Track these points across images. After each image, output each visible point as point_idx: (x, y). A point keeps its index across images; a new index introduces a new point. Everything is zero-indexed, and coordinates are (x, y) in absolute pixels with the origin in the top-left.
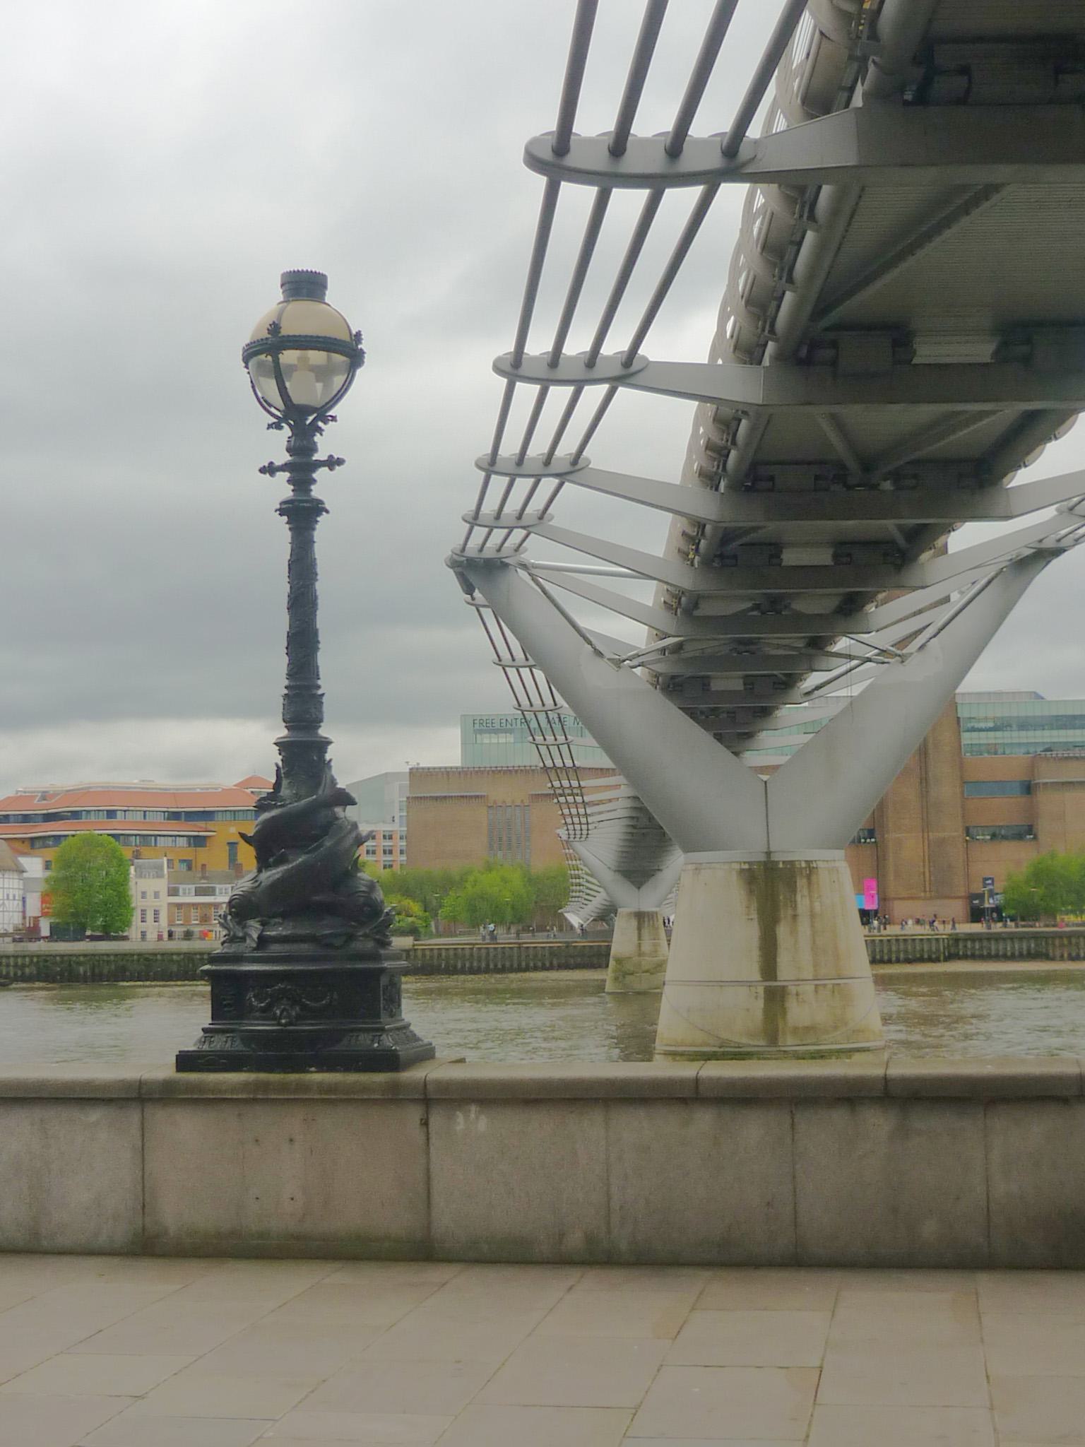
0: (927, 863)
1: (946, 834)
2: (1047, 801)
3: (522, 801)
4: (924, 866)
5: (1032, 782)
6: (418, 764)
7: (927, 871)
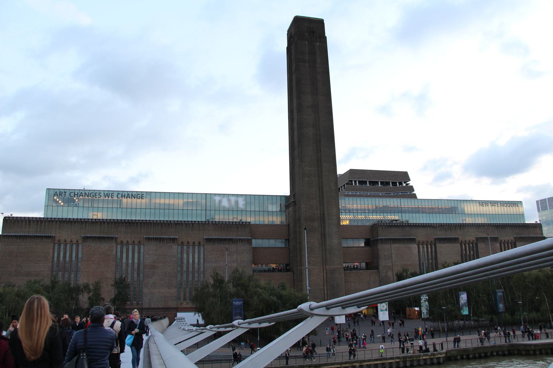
0: (325, 283)
1: (335, 266)
2: (383, 249)
3: (77, 241)
4: (324, 285)
5: (371, 239)
6: (11, 215)
7: (325, 288)
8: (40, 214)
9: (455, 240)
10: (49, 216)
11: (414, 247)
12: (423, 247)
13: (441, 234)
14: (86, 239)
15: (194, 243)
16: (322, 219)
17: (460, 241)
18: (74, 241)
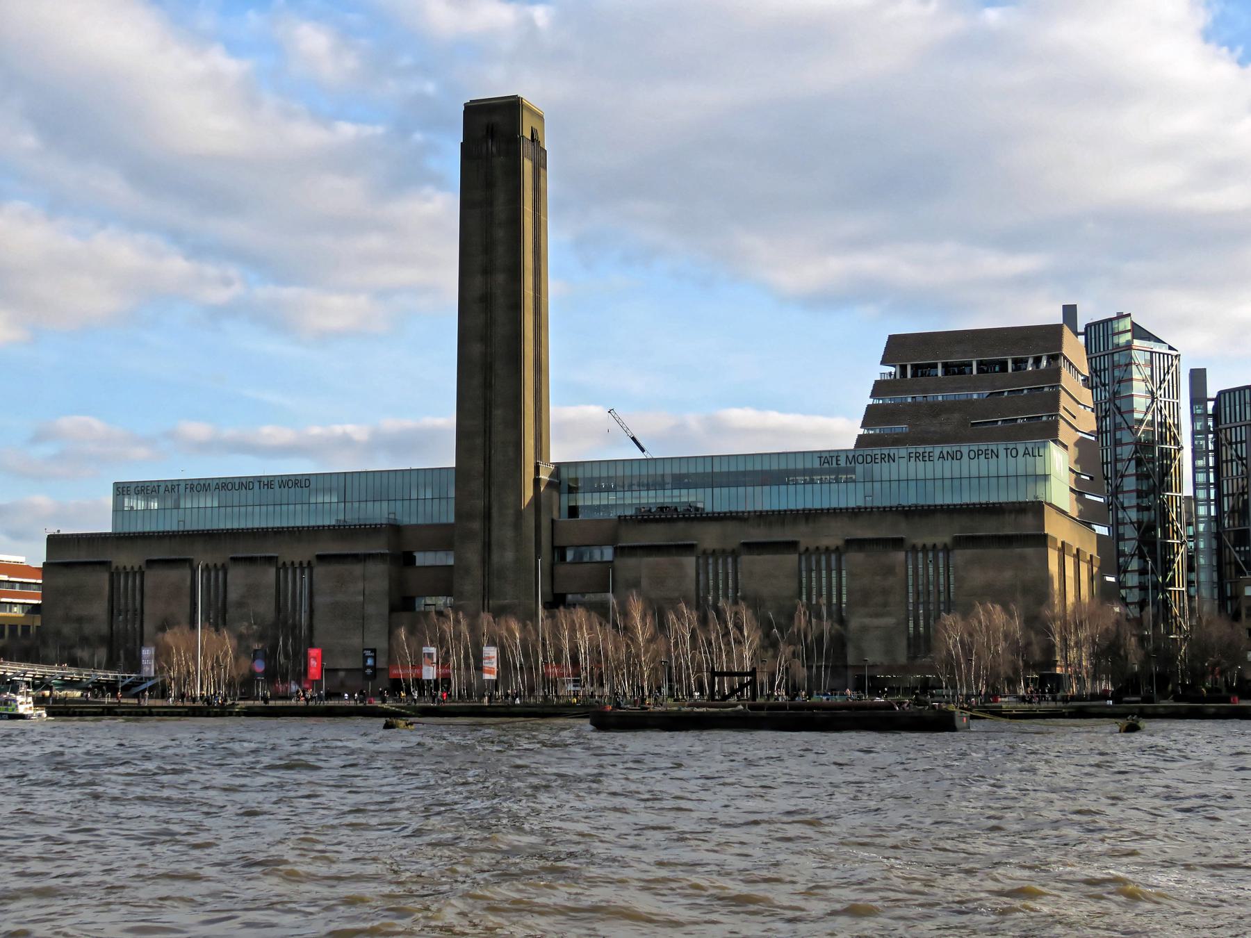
6: (59, 531)
8: (105, 526)
9: (791, 546)
10: (119, 530)
11: (689, 562)
12: (716, 563)
13: (758, 534)
14: (151, 563)
15: (301, 563)
16: (487, 516)
17: (802, 548)
18: (136, 569)
